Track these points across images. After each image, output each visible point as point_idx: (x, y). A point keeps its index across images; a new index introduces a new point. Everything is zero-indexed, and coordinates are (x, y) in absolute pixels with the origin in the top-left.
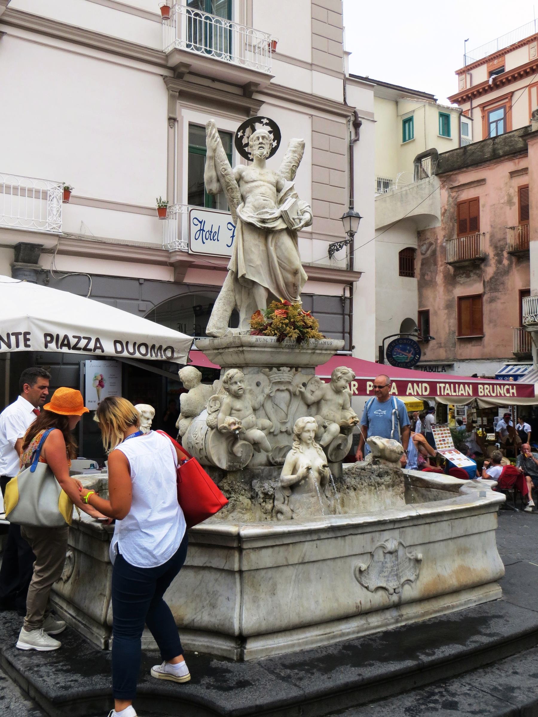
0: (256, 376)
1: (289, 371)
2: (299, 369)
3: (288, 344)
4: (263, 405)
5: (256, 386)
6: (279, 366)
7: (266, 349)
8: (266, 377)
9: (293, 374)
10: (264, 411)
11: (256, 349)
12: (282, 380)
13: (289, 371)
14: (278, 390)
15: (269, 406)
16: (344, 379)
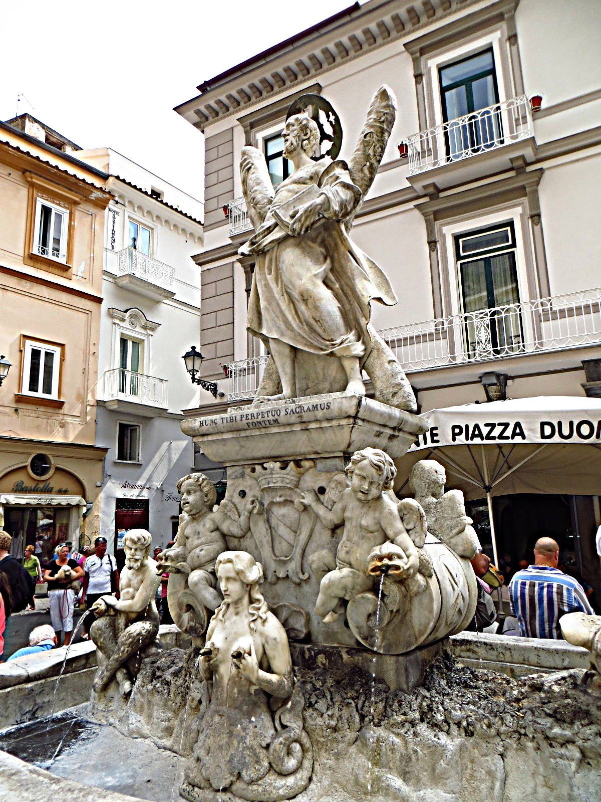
0: (240, 481)
1: (283, 468)
2: (306, 464)
3: (250, 421)
4: (250, 529)
5: (240, 498)
6: (262, 461)
7: (225, 436)
8: (254, 482)
9: (292, 473)
10: (252, 540)
11: (210, 438)
12: (271, 485)
13: (283, 468)
14: (272, 503)
15: (260, 529)
16: (356, 475)
